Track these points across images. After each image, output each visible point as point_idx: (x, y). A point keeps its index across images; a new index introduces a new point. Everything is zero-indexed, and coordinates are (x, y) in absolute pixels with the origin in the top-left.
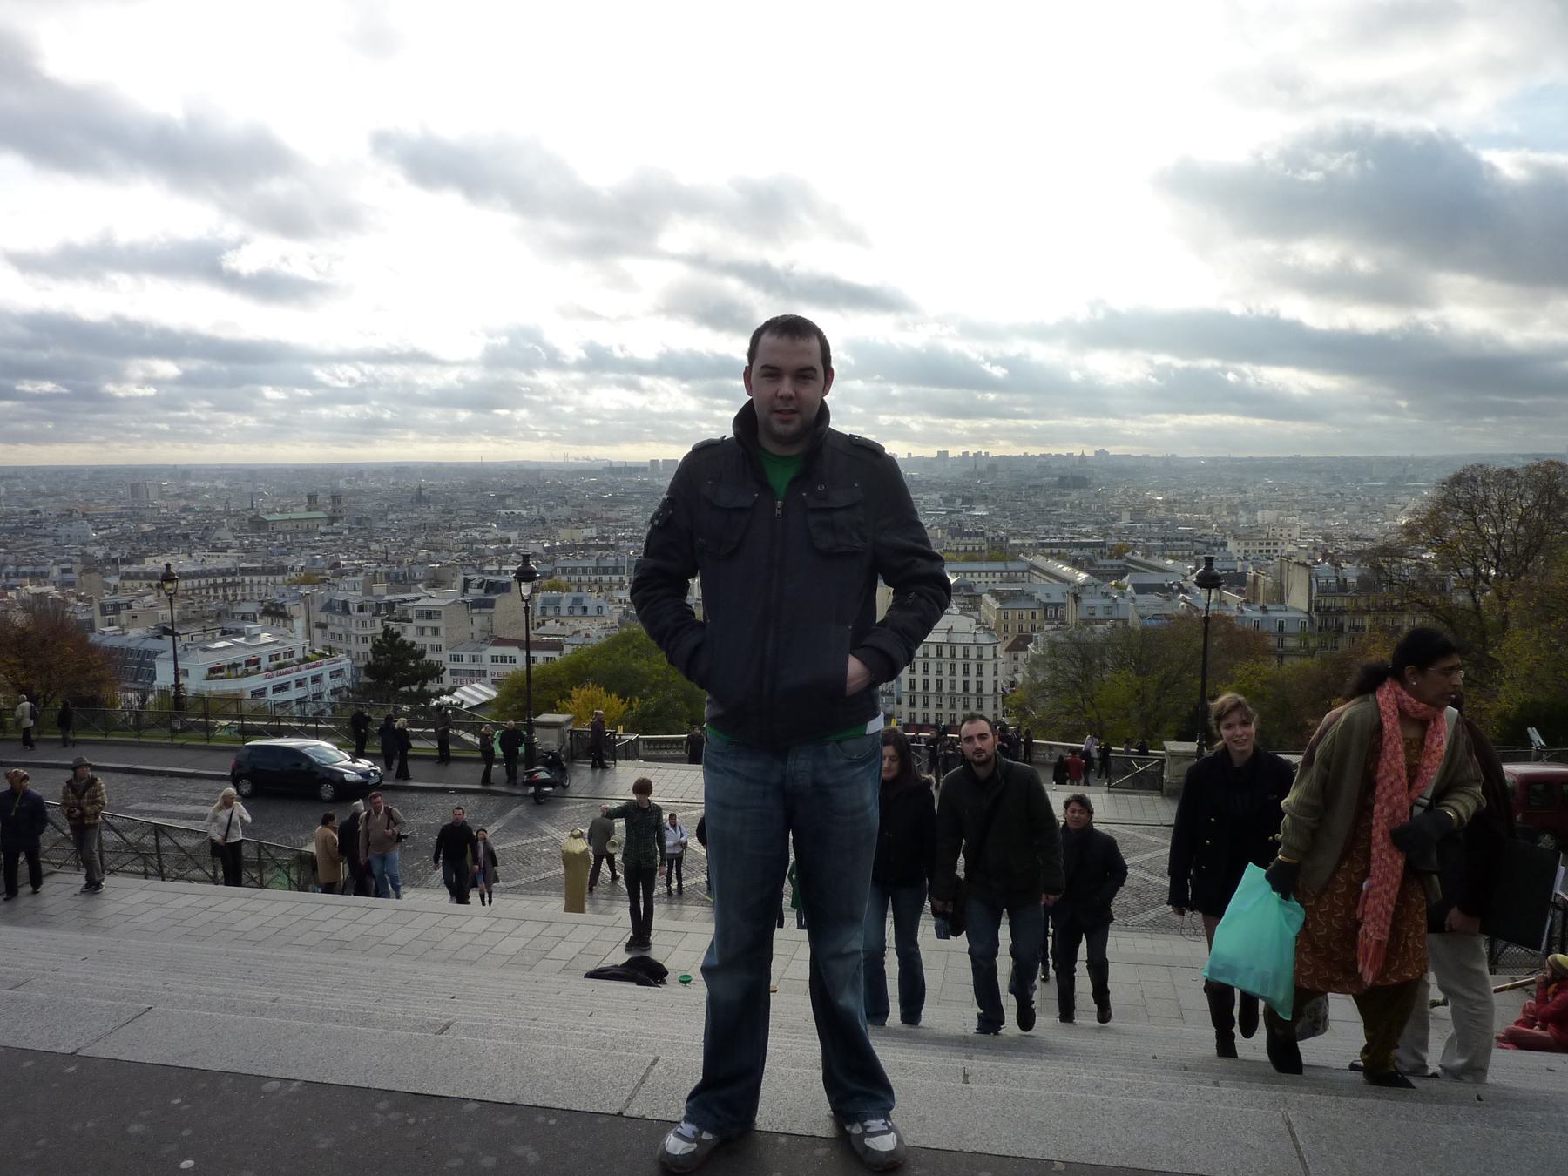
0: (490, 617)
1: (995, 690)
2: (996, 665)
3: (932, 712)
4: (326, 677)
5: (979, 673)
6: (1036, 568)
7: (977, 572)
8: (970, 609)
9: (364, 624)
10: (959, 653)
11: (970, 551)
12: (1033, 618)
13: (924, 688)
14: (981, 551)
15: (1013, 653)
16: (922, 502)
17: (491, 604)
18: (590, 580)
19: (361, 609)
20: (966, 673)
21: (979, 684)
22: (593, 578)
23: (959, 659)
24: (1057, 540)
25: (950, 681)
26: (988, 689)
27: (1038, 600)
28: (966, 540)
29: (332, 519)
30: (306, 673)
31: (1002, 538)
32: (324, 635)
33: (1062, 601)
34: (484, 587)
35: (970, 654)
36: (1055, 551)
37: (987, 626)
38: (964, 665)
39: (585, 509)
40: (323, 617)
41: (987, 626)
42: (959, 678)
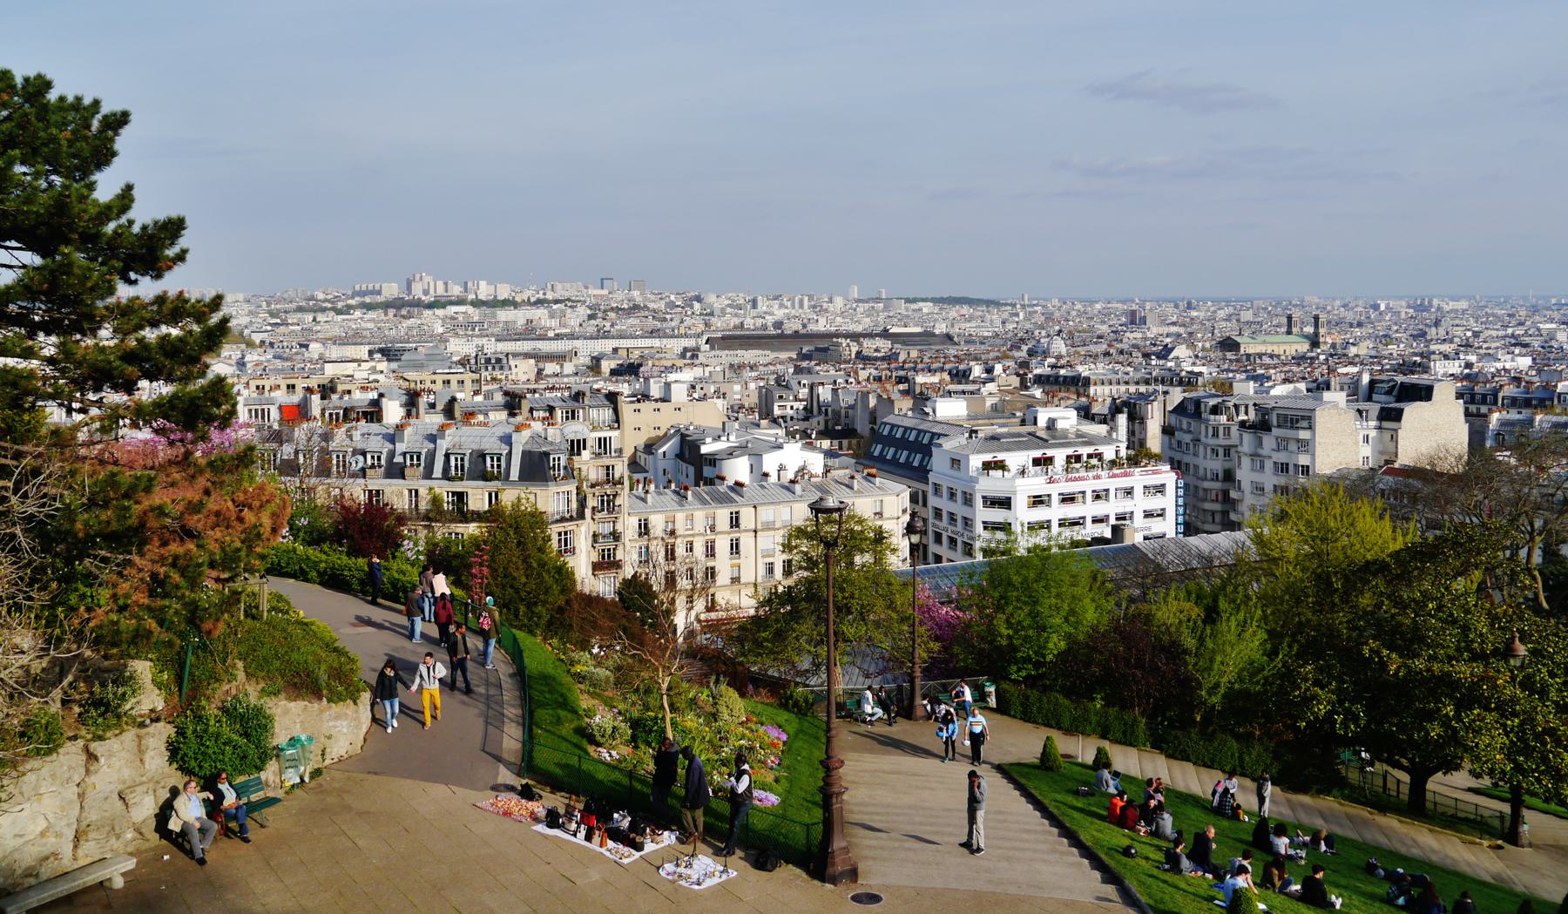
0: (1394, 439)
4: (1138, 491)
17: (1396, 416)
19: (1215, 410)
30: (1106, 481)
34: (1395, 393)
40: (1173, 420)
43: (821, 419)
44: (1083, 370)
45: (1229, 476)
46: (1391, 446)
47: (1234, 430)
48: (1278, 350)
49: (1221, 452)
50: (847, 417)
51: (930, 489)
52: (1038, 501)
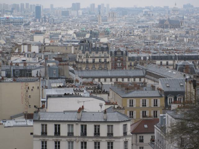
2: (126, 142)
6: (150, 74)
7: (103, 77)
8: (100, 93)
11: (97, 63)
12: (156, 105)
14: (106, 63)
15: (138, 136)
16: (60, 36)
24: (165, 54)
27: (159, 89)
28: (94, 54)
31: (122, 52)
33: (180, 89)
36: (164, 62)
41: (116, 106)
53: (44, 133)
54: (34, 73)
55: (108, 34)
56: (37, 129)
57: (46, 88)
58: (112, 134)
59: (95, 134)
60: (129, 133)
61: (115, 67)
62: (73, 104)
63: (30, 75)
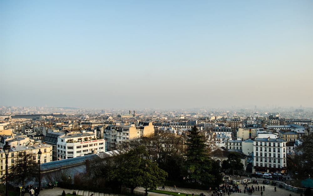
0: (143, 132)
1: (284, 157)
2: (284, 149)
3: (264, 163)
4: (98, 144)
5: (279, 151)
8: (275, 133)
9: (113, 132)
10: (272, 144)
13: (261, 155)
14: (278, 123)
17: (142, 128)
18: (178, 126)
19: (113, 128)
20: (274, 151)
21: (279, 155)
22: (179, 126)
23: (272, 147)
25: (269, 153)
26: (282, 156)
29: (134, 116)
30: (92, 142)
32: (105, 135)
33: (303, 132)
35: (276, 145)
36: (298, 123)
37: (281, 137)
38: (274, 149)
39: (187, 115)
40: (105, 131)
41: (281, 137)
42: (272, 153)
43: (36, 132)
44: (91, 122)
45: (115, 140)
46: (142, 134)
47: (116, 131)
48: (128, 117)
49: (114, 136)
50: (41, 132)
51: (57, 146)
52: (78, 147)
53: (257, 145)
54: (254, 126)
55: (278, 114)
56: (255, 143)
57: (258, 130)
58: (279, 146)
59: (274, 146)
60: (285, 146)
61: (280, 125)
62: (266, 136)
63: (253, 127)
